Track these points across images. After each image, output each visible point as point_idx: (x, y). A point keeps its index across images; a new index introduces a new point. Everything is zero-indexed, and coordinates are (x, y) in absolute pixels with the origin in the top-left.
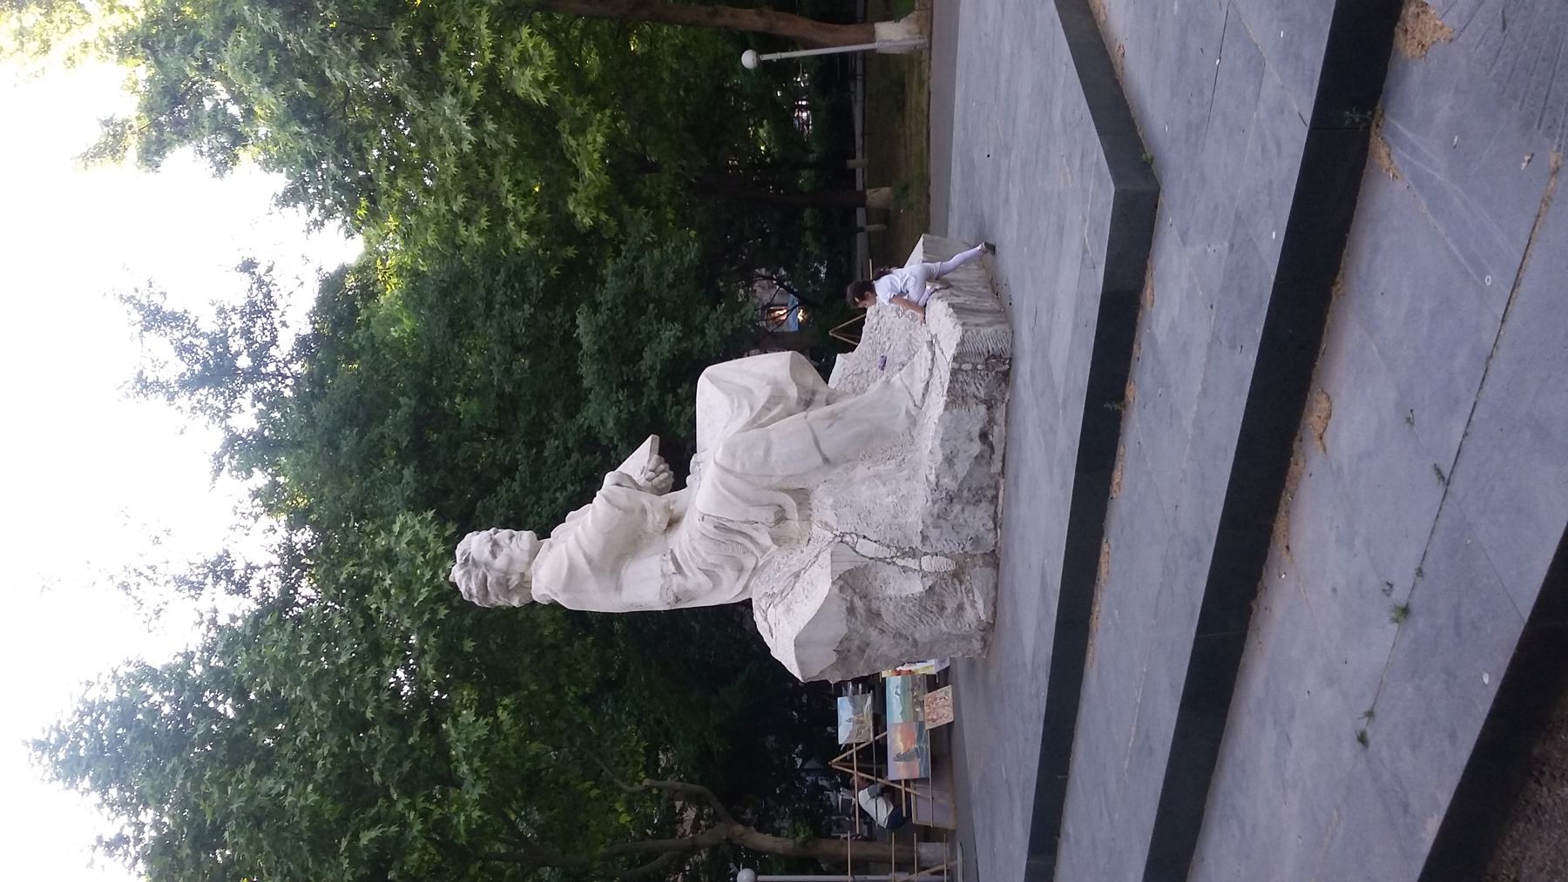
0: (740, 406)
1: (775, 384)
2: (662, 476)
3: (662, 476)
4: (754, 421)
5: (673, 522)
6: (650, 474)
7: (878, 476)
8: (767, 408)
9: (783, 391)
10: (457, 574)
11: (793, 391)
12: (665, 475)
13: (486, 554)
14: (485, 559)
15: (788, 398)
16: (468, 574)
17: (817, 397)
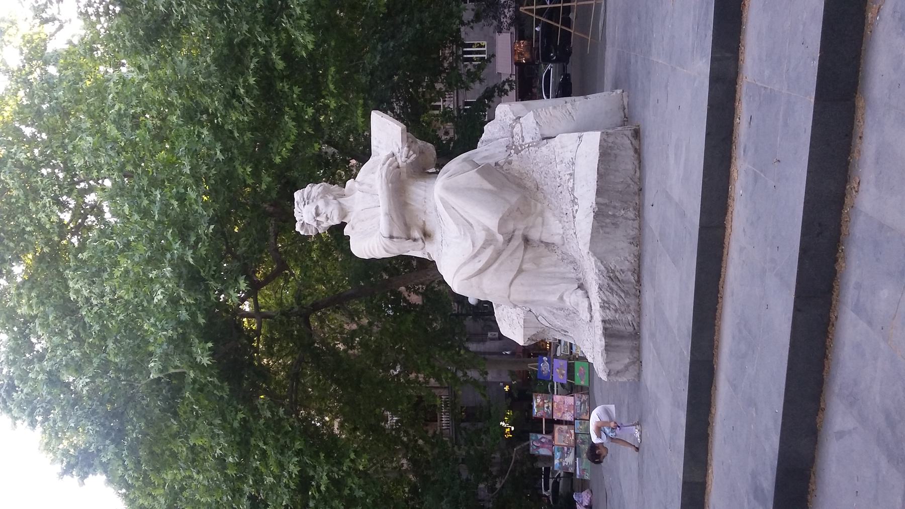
0: (465, 234)
1: (488, 230)
2: (412, 158)
3: (412, 158)
4: (475, 256)
5: (427, 235)
6: (404, 159)
7: (554, 314)
8: (483, 247)
9: (494, 235)
10: (298, 228)
11: (500, 238)
12: (415, 156)
13: (315, 224)
14: (311, 209)
15: (497, 241)
16: (307, 231)
17: (516, 233)
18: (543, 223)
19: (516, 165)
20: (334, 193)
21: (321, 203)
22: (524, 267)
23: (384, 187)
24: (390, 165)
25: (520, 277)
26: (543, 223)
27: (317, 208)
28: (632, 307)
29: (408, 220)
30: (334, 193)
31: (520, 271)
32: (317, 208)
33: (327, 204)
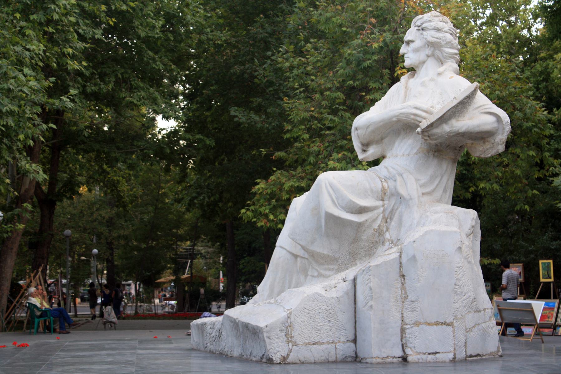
18: (313, 276)
19: (380, 250)
20: (438, 53)
21: (417, 44)
22: (299, 259)
23: (392, 114)
24: (415, 115)
25: (289, 256)
26: (313, 276)
27: (412, 41)
28: (212, 346)
29: (386, 140)
30: (438, 53)
31: (296, 256)
32: (412, 41)
33: (416, 50)
